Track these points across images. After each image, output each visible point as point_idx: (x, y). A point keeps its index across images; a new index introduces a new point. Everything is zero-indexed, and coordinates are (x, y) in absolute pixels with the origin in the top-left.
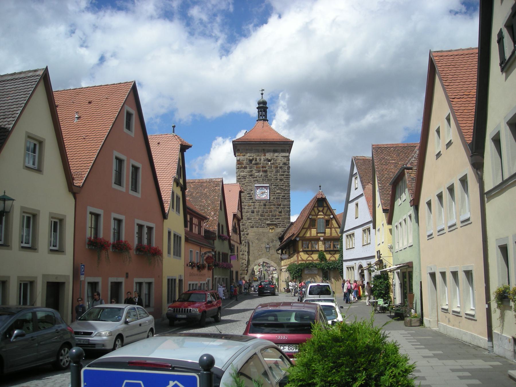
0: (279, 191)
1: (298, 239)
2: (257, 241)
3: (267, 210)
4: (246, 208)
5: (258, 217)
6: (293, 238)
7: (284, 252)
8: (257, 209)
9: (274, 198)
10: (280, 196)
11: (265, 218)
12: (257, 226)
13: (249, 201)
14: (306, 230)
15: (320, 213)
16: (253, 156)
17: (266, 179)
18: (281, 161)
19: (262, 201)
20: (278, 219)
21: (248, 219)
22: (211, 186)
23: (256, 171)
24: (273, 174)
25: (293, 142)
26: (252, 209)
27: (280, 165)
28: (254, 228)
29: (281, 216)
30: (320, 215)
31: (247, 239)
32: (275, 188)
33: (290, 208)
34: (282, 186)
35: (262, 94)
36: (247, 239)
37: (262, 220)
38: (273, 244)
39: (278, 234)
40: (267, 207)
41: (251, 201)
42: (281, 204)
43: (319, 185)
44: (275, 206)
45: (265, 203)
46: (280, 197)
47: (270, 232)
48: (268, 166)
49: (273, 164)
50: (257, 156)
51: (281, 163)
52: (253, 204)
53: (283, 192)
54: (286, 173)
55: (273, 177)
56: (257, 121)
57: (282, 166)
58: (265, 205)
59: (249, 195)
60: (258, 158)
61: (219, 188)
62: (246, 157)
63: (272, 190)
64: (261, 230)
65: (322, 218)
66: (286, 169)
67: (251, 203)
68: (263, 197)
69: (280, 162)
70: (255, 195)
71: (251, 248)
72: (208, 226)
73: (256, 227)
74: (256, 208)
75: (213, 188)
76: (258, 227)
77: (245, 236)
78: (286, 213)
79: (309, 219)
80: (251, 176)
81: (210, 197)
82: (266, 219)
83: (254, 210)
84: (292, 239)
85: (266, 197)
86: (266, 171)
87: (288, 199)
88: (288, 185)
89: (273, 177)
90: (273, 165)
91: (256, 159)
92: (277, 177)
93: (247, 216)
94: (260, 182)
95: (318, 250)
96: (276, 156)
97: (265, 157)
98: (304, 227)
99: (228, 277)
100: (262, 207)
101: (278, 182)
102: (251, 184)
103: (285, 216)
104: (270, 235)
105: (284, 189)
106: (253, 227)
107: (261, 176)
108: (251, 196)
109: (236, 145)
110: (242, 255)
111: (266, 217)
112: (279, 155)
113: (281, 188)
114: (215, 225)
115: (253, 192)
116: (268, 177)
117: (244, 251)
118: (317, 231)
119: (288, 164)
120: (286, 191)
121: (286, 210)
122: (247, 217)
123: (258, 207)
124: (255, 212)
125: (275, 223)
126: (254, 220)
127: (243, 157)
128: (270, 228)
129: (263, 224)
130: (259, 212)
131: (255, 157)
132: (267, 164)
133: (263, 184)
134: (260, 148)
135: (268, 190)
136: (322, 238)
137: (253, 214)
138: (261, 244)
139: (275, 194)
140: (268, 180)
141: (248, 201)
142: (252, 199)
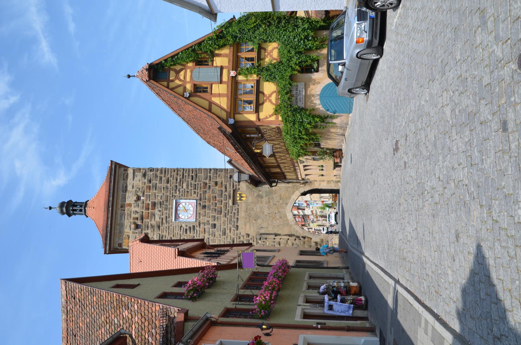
0: (185, 185)
1: (231, 121)
2: (259, 221)
3: (212, 203)
4: (208, 236)
5: (222, 219)
6: (229, 130)
7: (258, 151)
8: (210, 219)
9: (195, 192)
10: (191, 184)
11: (224, 207)
12: (235, 220)
13: (197, 231)
14: (213, 105)
15: (182, 77)
16: (131, 223)
17: (164, 204)
18: (140, 181)
19: (198, 212)
20: (226, 188)
21: (224, 234)
22: (73, 309)
23: (153, 220)
24: (158, 193)
25: (112, 161)
26: (210, 227)
27: (146, 183)
28: (238, 224)
29: (222, 183)
30: (185, 77)
31: (255, 236)
32: (179, 191)
33: (210, 169)
34: (177, 180)
35: (50, 208)
36: (255, 236)
37: (227, 212)
38: (264, 195)
39: (249, 188)
40: (207, 204)
41: (198, 228)
42: (204, 183)
43: (126, 78)
44: (206, 191)
45: (202, 206)
46: (193, 183)
47: (247, 200)
48: (146, 200)
49: (144, 194)
50: (131, 217)
51: (144, 181)
52: (201, 225)
53: (185, 179)
54: (158, 173)
55: (163, 194)
56: (87, 217)
57: (148, 180)
58: (204, 207)
59: (188, 231)
60: (133, 216)
61: (77, 291)
62: (131, 235)
63: (182, 195)
64: (242, 214)
65: (191, 72)
66: (152, 173)
67: (200, 228)
68: (192, 209)
69: (141, 181)
70: (189, 222)
71: (271, 230)
72: (153, 331)
73: (237, 222)
74: (208, 221)
75: (78, 306)
76: (238, 219)
77: (251, 239)
78: (218, 175)
79: (191, 99)
80: (159, 227)
81: (93, 315)
82: (226, 206)
83: (212, 224)
84: (230, 131)
85: (193, 204)
86: (154, 204)
87: (196, 171)
88: (176, 171)
89: (163, 194)
90: (145, 193)
91: (134, 219)
92: (164, 188)
93: (220, 235)
94: (169, 214)
95: (256, 82)
96: (133, 187)
97: (133, 206)
98: (207, 108)
99: (308, 272)
100: (207, 211)
101: (170, 186)
102: (172, 228)
103: (223, 177)
104: (250, 200)
105: (181, 177)
106: (237, 226)
107: (160, 211)
108: (190, 228)
109: (112, 249)
110: (280, 245)
111: (222, 206)
112: (131, 184)
113: (180, 181)
114: (150, 311)
115: (184, 225)
116: (163, 201)
117: (274, 242)
118: (215, 83)
119: (146, 170)
120: (185, 174)
121: (213, 175)
122: (221, 235)
123: (207, 217)
124: (215, 222)
125: (232, 192)
126: (226, 224)
127: (131, 238)
128: (240, 200)
129: (234, 211)
130: (215, 216)
131: (132, 221)
132: (143, 202)
133: (172, 208)
134: (119, 212)
135: (181, 201)
136: (233, 73)
137: (218, 225)
138: (263, 214)
139: (188, 192)
140: (167, 201)
141: (197, 233)
142: (194, 227)
